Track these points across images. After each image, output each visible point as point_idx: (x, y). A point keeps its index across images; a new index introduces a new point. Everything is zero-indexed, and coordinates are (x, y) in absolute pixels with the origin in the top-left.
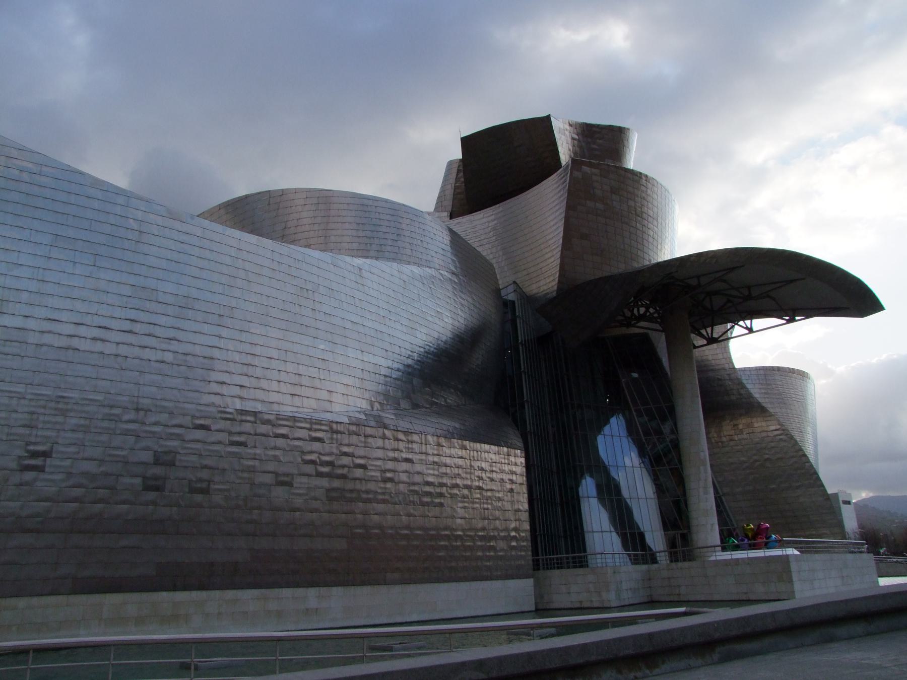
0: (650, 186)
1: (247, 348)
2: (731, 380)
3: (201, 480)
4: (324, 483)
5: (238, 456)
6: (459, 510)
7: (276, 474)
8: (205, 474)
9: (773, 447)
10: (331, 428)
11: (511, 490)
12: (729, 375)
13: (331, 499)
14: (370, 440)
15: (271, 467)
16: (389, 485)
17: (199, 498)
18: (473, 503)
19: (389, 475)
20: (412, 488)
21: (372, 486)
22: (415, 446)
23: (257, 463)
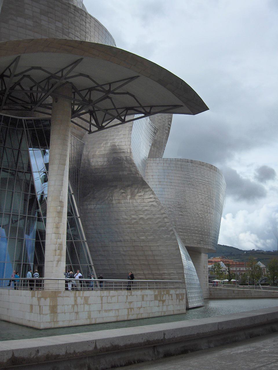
0: (78, 14)
2: (127, 160)
9: (146, 210)
12: (126, 157)
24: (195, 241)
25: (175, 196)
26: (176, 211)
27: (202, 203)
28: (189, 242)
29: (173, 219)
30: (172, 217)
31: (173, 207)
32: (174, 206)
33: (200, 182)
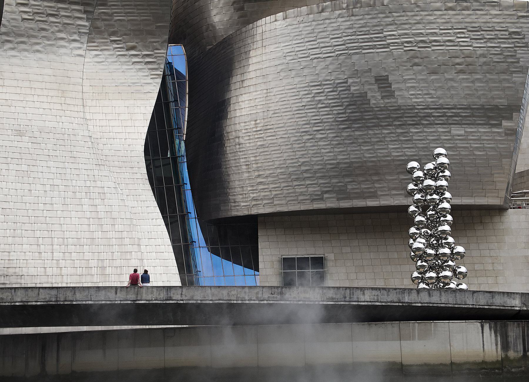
24: (301, 198)
25: (248, 109)
26: (252, 141)
27: (322, 104)
28: (283, 202)
29: (244, 160)
30: (242, 155)
31: (245, 133)
32: (246, 131)
33: (312, 57)
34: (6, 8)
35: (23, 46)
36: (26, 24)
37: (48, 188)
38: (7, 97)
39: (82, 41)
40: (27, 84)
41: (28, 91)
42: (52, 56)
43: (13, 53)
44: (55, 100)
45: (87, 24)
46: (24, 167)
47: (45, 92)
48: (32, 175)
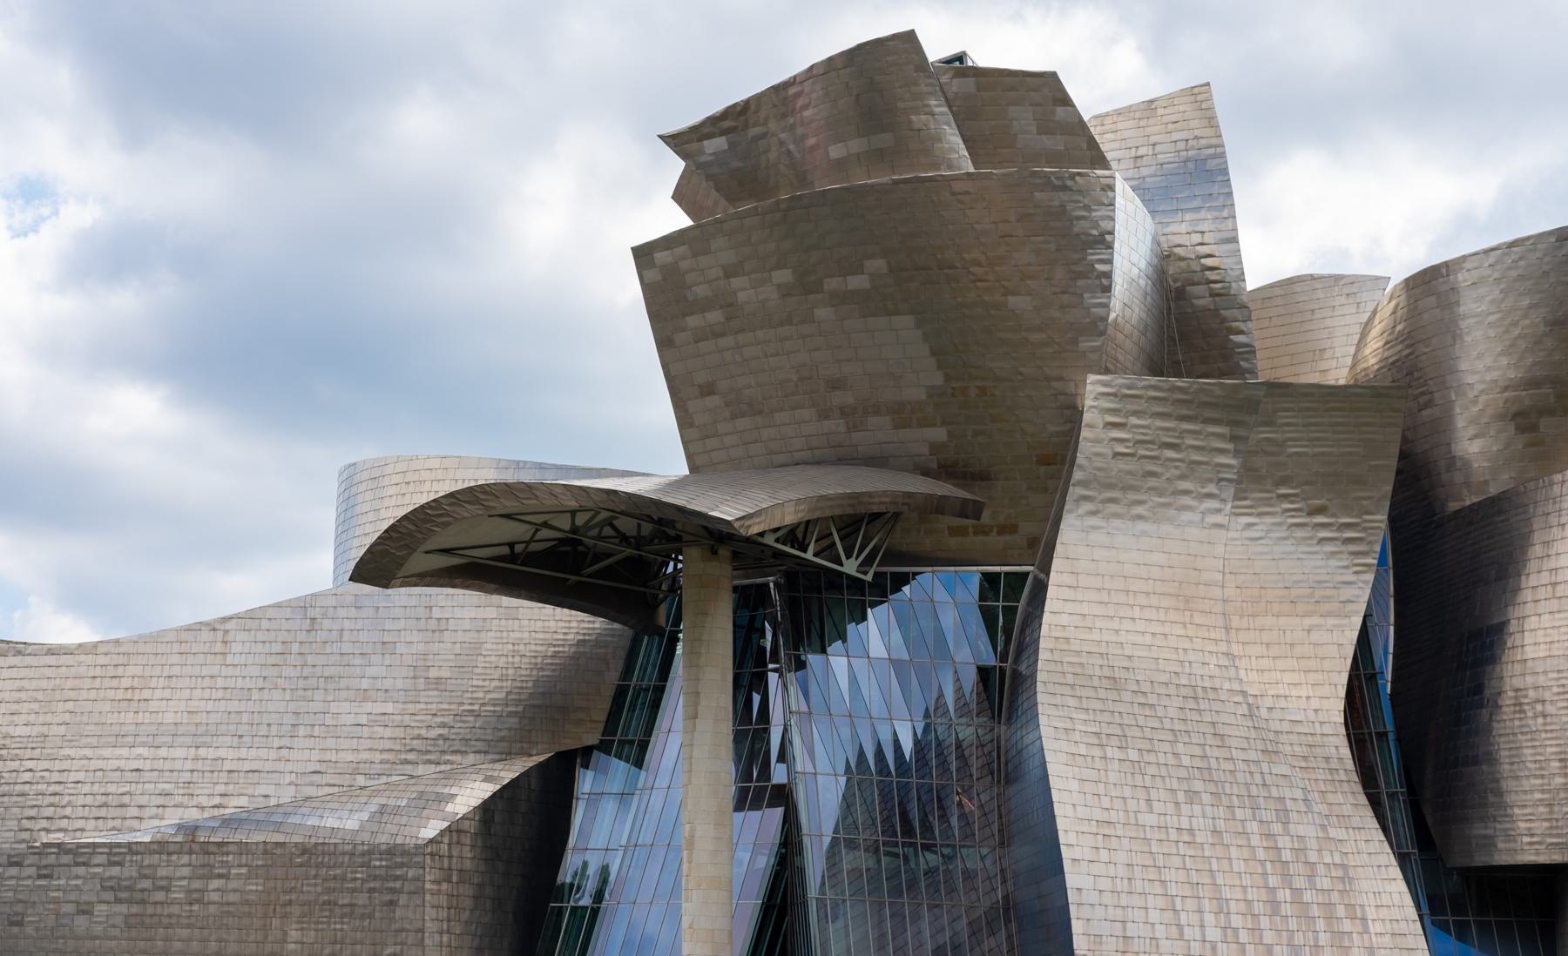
1: (56, 777)
3: (16, 914)
4: (123, 908)
5: (46, 889)
6: (293, 933)
7: (78, 903)
8: (19, 908)
10: (130, 850)
11: (391, 903)
13: (129, 927)
14: (174, 857)
15: (73, 897)
16: (195, 907)
17: (15, 930)
18: (317, 923)
19: (195, 896)
20: (226, 908)
21: (175, 909)
22: (230, 858)
23: (60, 894)
34: (1085, 433)
35: (1112, 508)
36: (1122, 465)
37: (1181, 797)
38: (1085, 609)
39: (1223, 496)
40: (1119, 584)
41: (1122, 598)
42: (1166, 528)
43: (1094, 521)
44: (1173, 616)
45: (1233, 462)
46: (1133, 755)
47: (1154, 600)
48: (1152, 770)
